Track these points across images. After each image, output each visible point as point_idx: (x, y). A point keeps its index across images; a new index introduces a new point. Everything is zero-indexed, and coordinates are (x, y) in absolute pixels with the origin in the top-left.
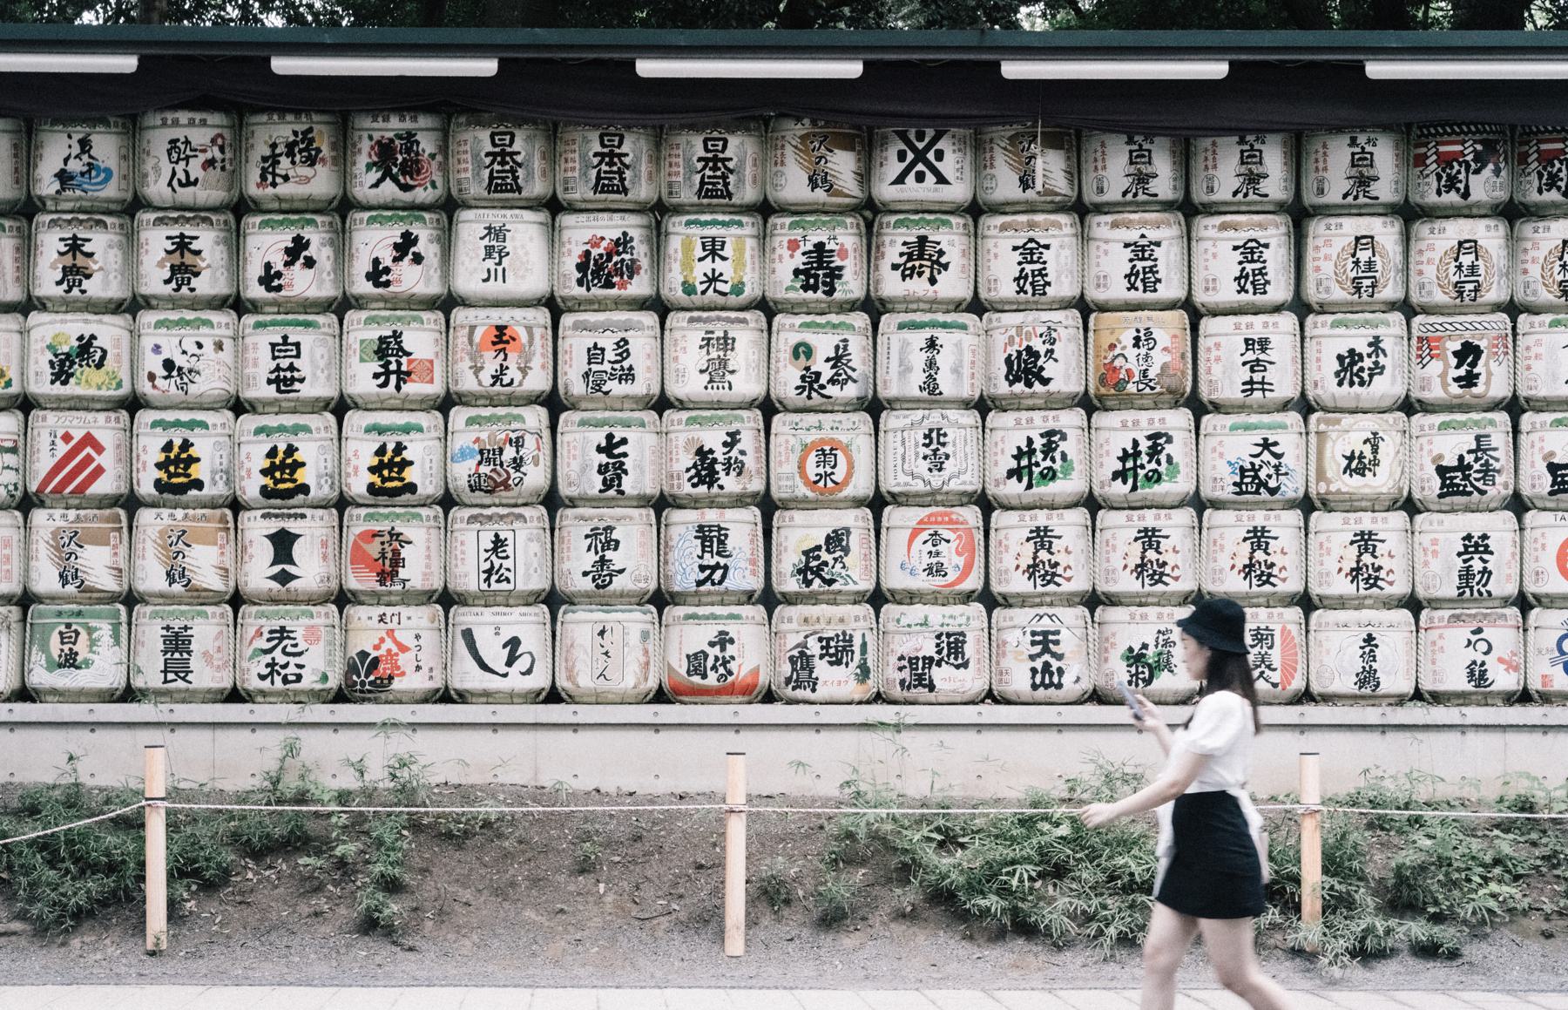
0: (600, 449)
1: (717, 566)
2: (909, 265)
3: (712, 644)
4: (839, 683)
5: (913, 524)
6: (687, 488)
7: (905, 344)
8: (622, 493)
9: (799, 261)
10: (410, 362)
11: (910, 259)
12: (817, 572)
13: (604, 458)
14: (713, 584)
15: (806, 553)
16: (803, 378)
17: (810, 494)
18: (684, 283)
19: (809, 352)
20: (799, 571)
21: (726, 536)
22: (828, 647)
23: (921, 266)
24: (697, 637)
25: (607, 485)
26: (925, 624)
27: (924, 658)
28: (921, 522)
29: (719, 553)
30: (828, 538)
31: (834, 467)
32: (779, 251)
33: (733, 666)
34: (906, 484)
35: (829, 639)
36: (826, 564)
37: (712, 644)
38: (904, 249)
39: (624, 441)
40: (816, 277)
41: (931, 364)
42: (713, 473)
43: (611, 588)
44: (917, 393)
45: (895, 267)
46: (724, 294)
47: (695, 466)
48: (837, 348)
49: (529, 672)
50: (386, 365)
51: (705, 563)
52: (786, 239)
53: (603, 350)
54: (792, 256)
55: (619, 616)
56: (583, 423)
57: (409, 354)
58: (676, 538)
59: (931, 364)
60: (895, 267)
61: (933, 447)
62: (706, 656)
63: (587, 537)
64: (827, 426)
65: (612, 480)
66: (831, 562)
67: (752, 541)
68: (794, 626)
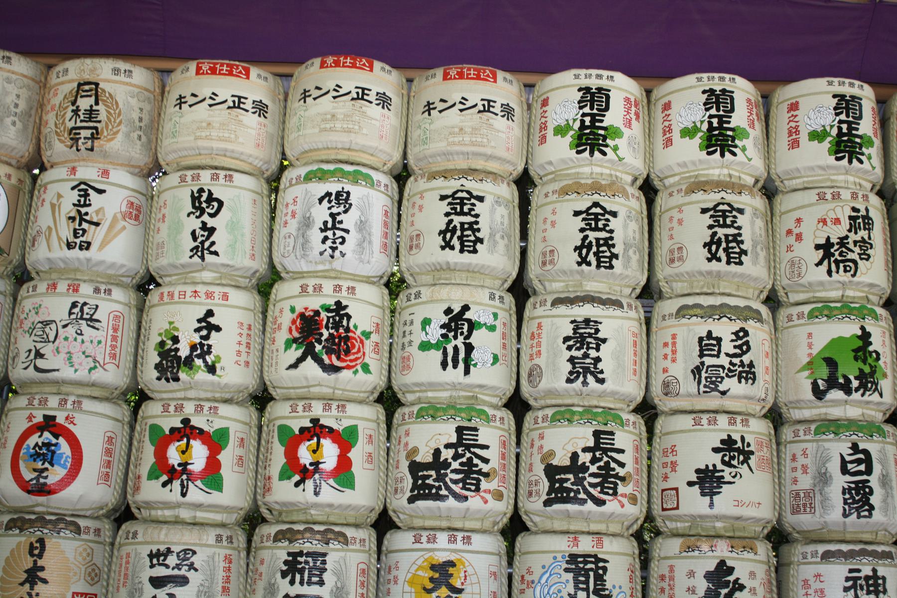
21: (605, 569)
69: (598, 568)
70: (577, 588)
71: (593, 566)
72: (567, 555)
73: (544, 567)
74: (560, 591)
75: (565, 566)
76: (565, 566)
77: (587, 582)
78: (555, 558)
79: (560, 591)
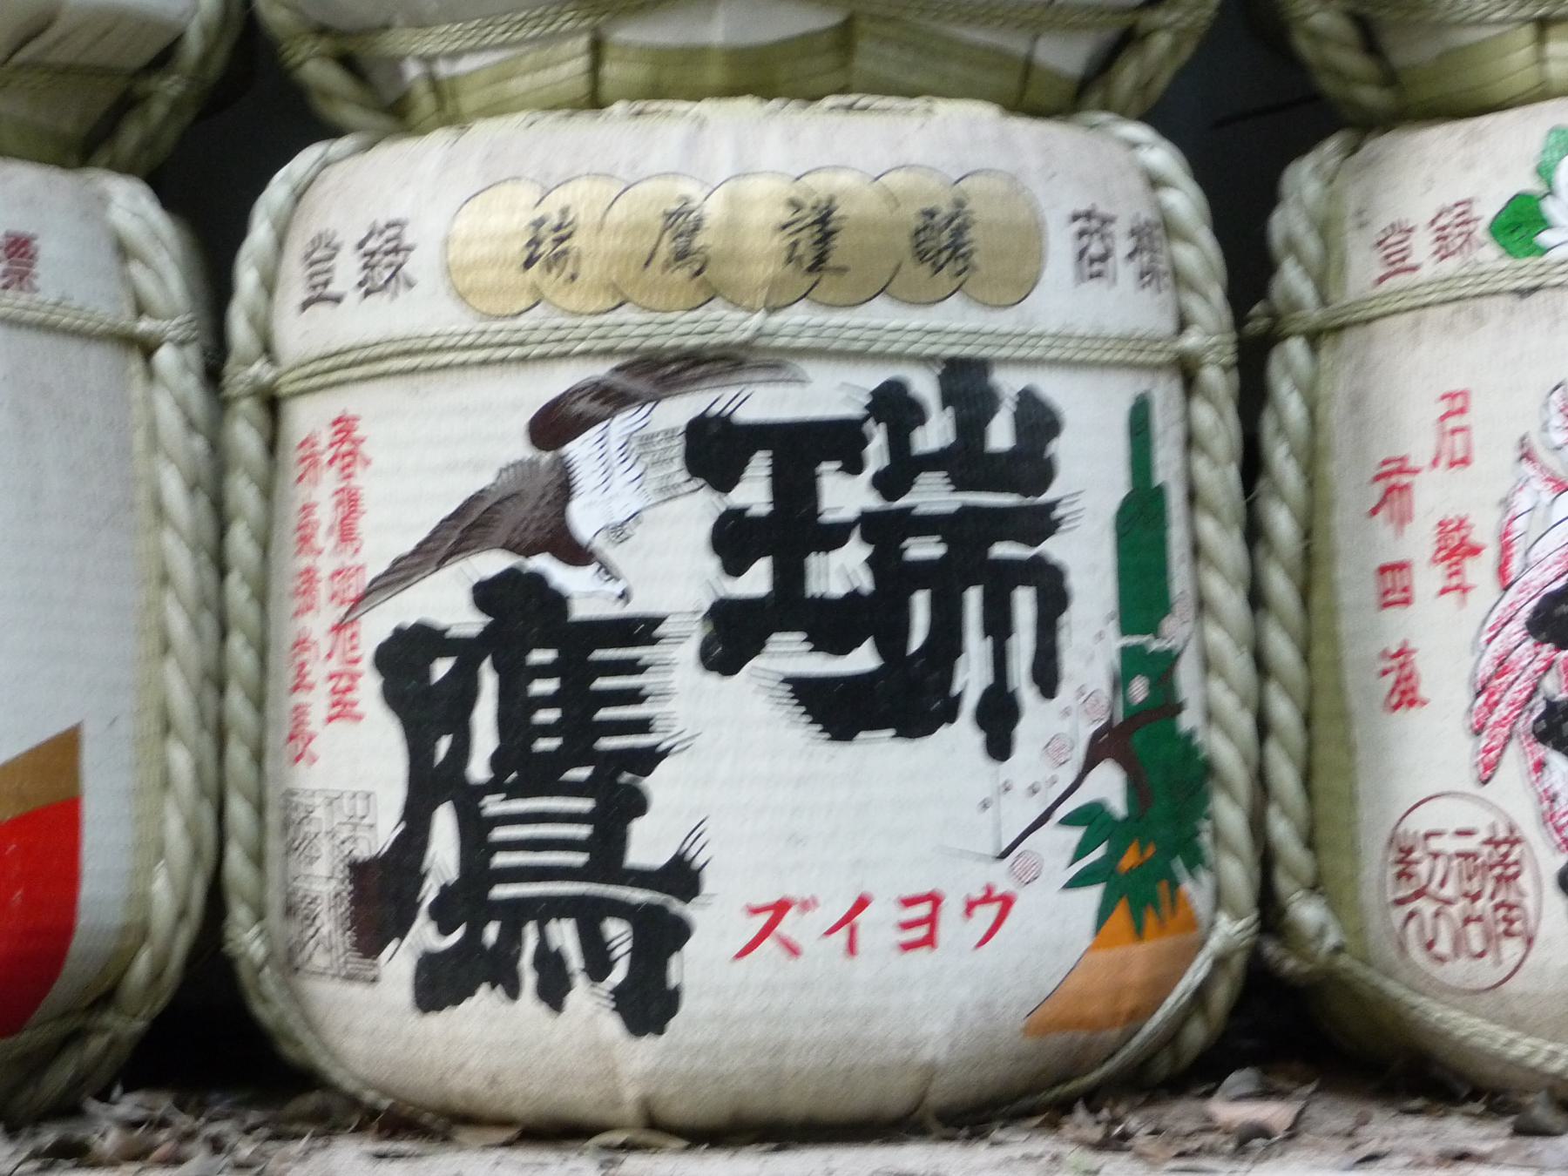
4: (924, 922)
22: (793, 531)
35: (804, 448)
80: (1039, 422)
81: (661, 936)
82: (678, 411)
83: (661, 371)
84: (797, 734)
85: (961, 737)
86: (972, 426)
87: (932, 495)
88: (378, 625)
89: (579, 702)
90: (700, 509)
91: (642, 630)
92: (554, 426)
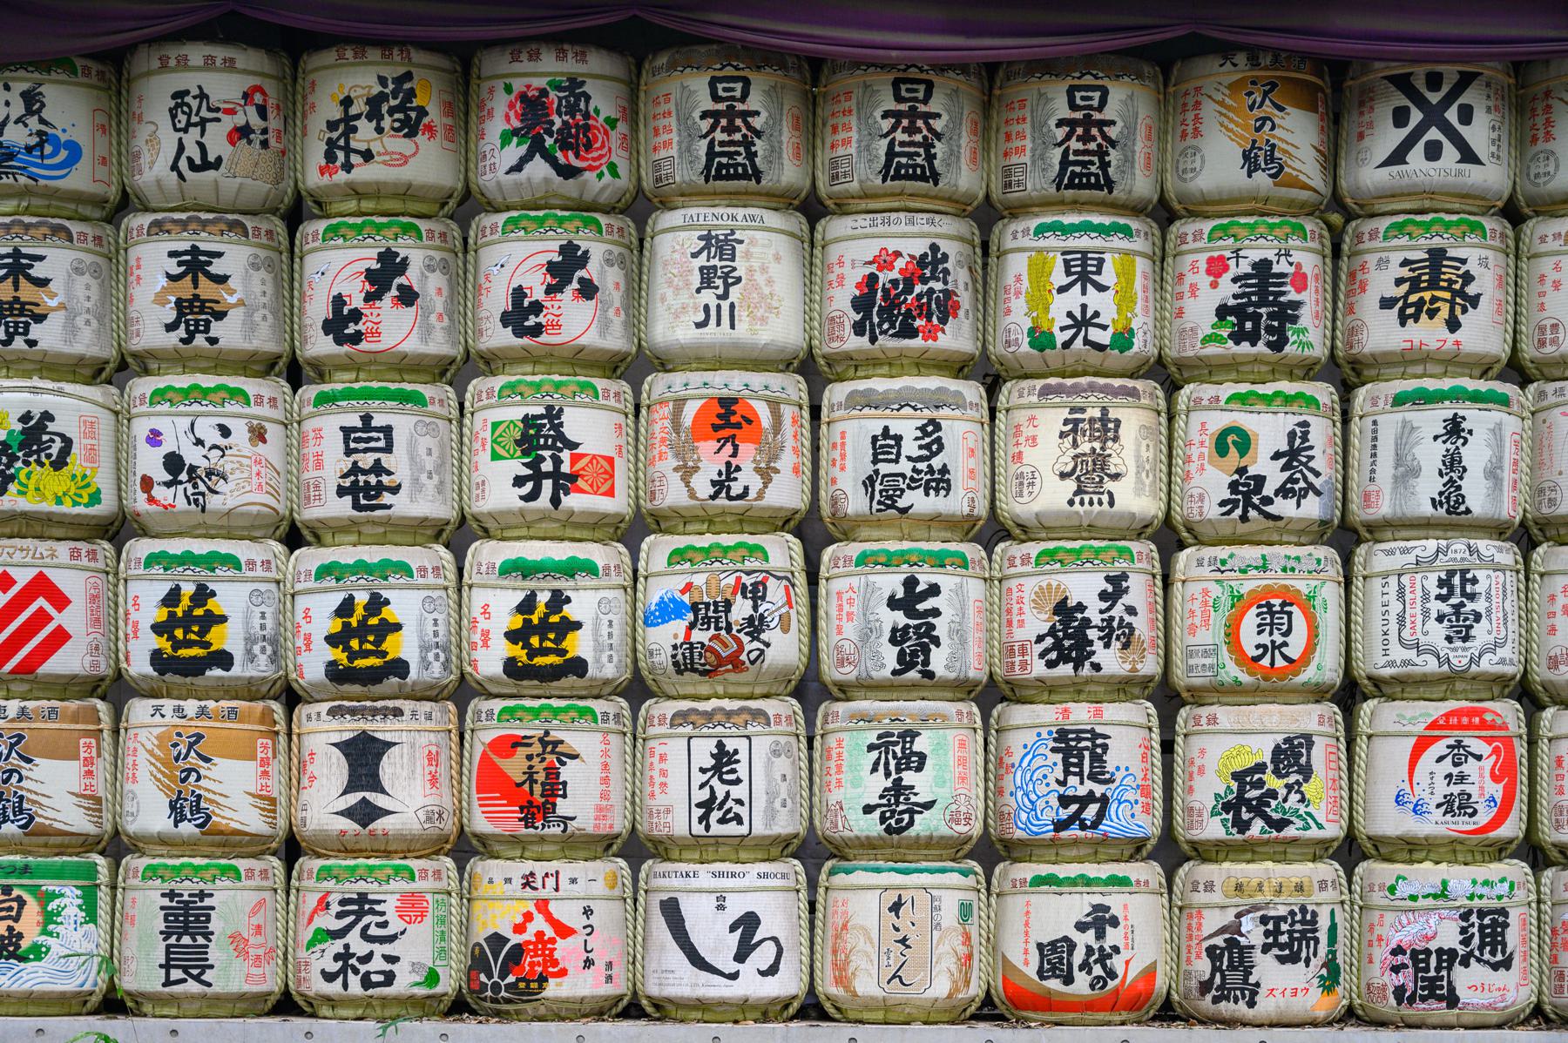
0: (893, 603)
1: (1091, 797)
2: (1413, 298)
3: (1081, 927)
4: (1295, 993)
5: (1420, 729)
6: (1038, 668)
7: (1408, 429)
8: (929, 675)
9: (1227, 290)
10: (575, 459)
11: (1415, 285)
12: (1259, 809)
13: (900, 618)
14: (1083, 827)
15: (1236, 776)
16: (1233, 487)
17: (1245, 678)
18: (1032, 331)
19: (1244, 442)
20: (1227, 807)
21: (1105, 747)
22: (1277, 932)
23: (1434, 299)
24: (1058, 915)
25: (905, 662)
26: (1443, 893)
27: (1440, 951)
28: (1433, 725)
29: (1093, 777)
30: (1277, 751)
31: (1287, 633)
32: (1190, 278)
33: (1117, 963)
34: (1406, 663)
35: (1279, 920)
36: (1273, 794)
37: (1081, 927)
38: (1405, 272)
39: (934, 590)
40: (1256, 318)
41: (1453, 463)
42: (1083, 643)
43: (912, 832)
44: (1428, 510)
45: (1387, 303)
46: (1100, 348)
47: (1052, 632)
48: (1292, 436)
49: (772, 970)
50: (534, 465)
51: (1070, 792)
52: (1202, 259)
53: (898, 439)
54: (1214, 285)
55: (925, 879)
56: (864, 560)
57: (573, 446)
58: (1018, 753)
59: (1453, 463)
60: (1387, 303)
61: (1454, 601)
62: (1072, 946)
63: (871, 748)
64: (1276, 565)
65: (914, 654)
66: (1282, 792)
67: (1144, 758)
68: (1216, 897)
69: (1095, 746)
70: (1067, 773)
71: (1089, 744)
72: (1054, 729)
73: (1025, 746)
74: (1045, 776)
75: (1052, 744)
76: (1052, 744)
77: (1080, 765)
78: (1039, 735)
79: (1045, 776)
80: (1314, 914)
81: (1254, 993)
82: (1260, 914)
83: (1255, 908)
84: (1276, 963)
85: (1302, 964)
86: (1304, 916)
87: (1298, 927)
88: (1206, 944)
89: (1241, 957)
90: (1263, 928)
91: (1253, 947)
92: (1239, 916)
